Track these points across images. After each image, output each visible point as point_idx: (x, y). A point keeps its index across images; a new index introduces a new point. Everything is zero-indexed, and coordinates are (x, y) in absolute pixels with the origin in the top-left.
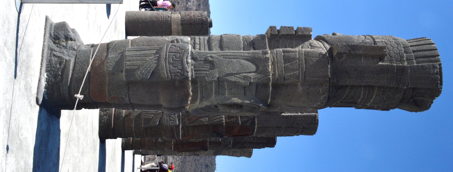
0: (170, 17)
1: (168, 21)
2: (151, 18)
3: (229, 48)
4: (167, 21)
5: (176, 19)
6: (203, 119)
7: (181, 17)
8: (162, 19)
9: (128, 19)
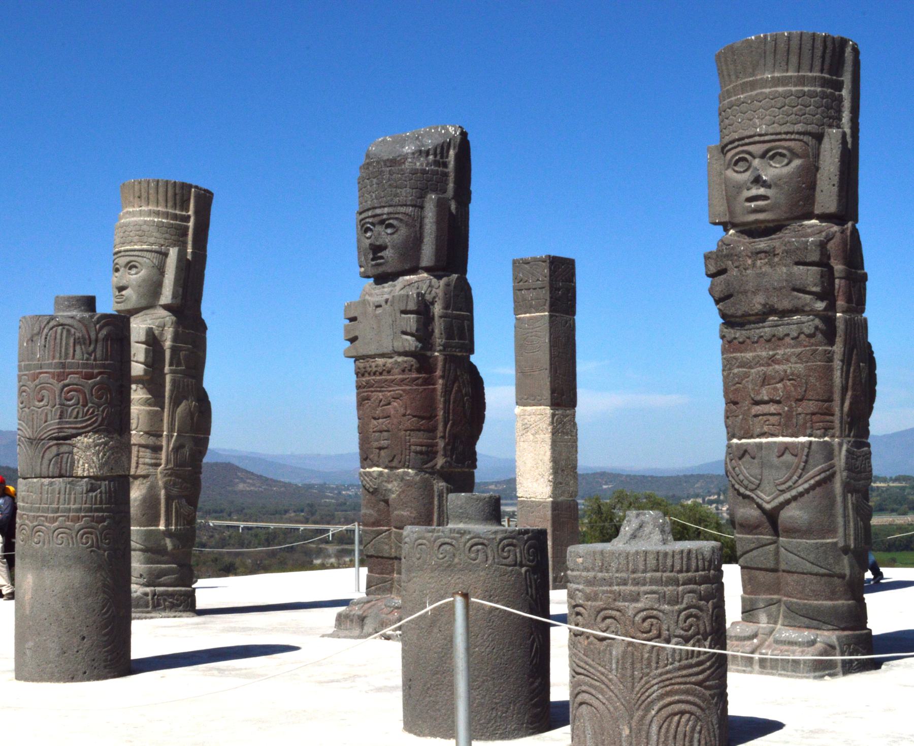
0: (93, 481)
2: (100, 567)
4: (110, 496)
5: (103, 458)
7: (95, 433)
8: (102, 520)
9: (105, 667)
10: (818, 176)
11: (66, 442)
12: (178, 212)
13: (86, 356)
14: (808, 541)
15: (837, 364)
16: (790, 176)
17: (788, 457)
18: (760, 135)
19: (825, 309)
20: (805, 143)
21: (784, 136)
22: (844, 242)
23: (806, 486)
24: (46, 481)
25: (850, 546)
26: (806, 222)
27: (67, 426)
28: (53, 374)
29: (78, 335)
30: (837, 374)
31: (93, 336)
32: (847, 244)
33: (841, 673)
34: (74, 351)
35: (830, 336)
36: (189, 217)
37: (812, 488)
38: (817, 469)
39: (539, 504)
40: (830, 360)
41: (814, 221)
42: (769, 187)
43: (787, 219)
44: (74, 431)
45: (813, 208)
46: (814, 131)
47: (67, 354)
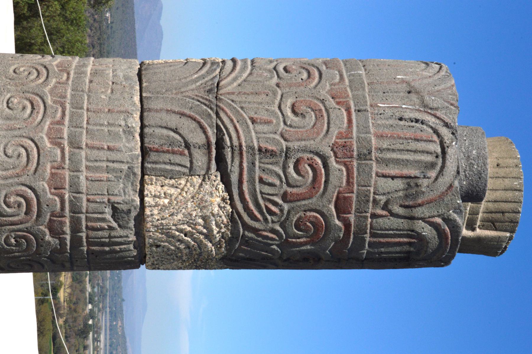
0: (134, 214)
1: (117, 248)
4: (103, 244)
5: (181, 231)
7: (232, 218)
11: (213, 162)
12: (480, 216)
13: (383, 199)
24: (136, 124)
27: (245, 165)
28: (348, 134)
29: (425, 182)
31: (418, 212)
34: (393, 178)
36: (473, 229)
44: (234, 178)
47: (387, 162)
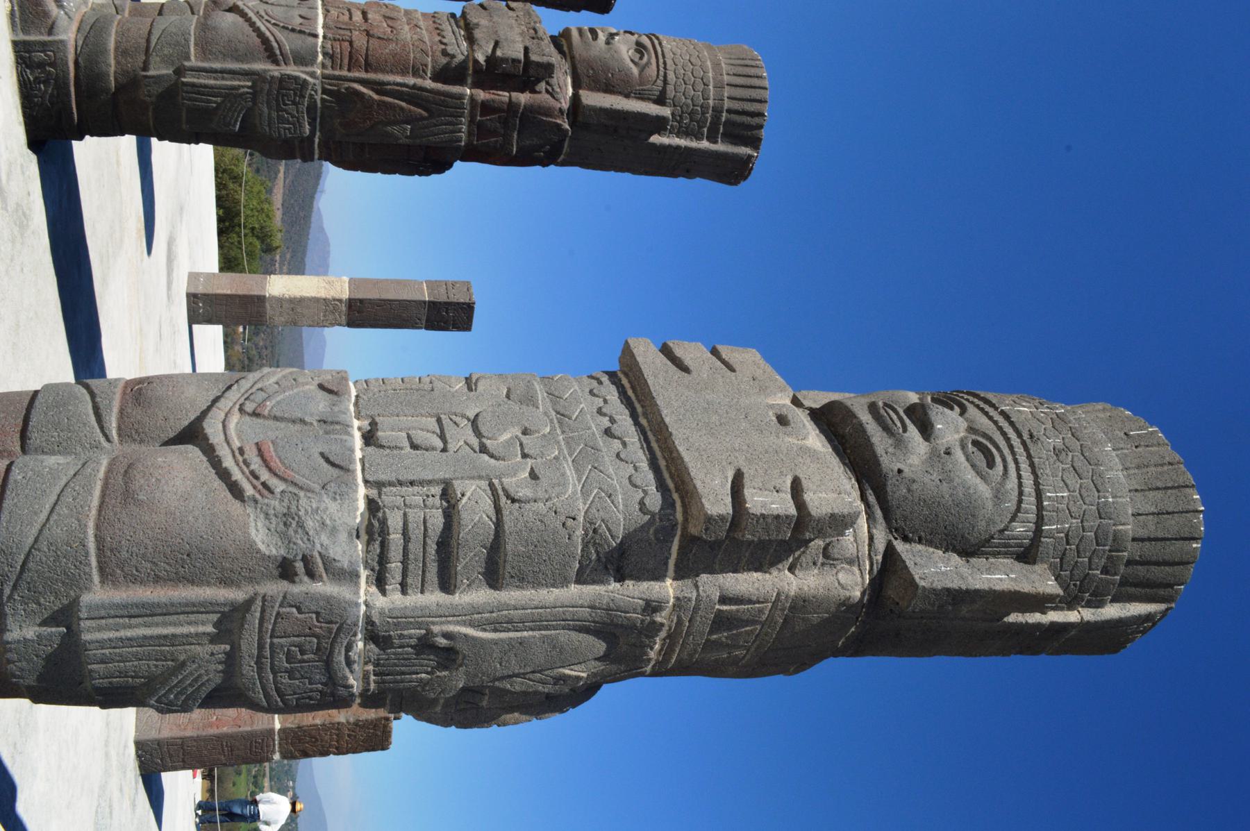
3: (522, 580)
6: (395, 130)
10: (620, 97)
14: (193, 27)
15: (411, 81)
16: (622, 60)
17: (300, 20)
18: (660, 44)
19: (476, 62)
20: (656, 81)
21: (661, 61)
22: (548, 112)
23: (263, 28)
25: (185, 77)
26: (569, 80)
30: (399, 79)
32: (547, 116)
33: (16, 39)
35: (443, 75)
37: (260, 34)
38: (282, 38)
39: (264, 288)
40: (416, 73)
41: (570, 91)
42: (608, 43)
43: (572, 58)
45: (585, 89)
46: (668, 92)
